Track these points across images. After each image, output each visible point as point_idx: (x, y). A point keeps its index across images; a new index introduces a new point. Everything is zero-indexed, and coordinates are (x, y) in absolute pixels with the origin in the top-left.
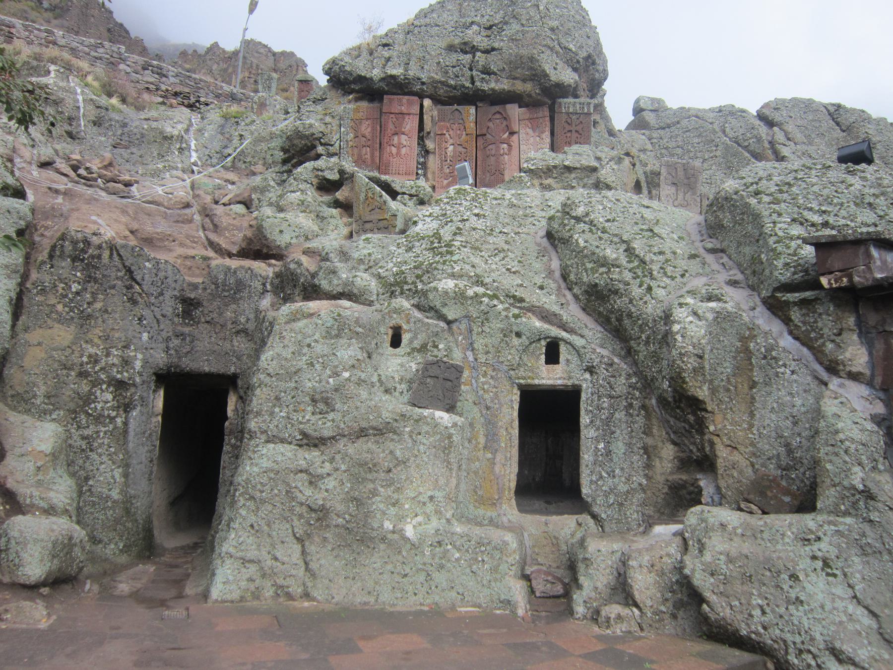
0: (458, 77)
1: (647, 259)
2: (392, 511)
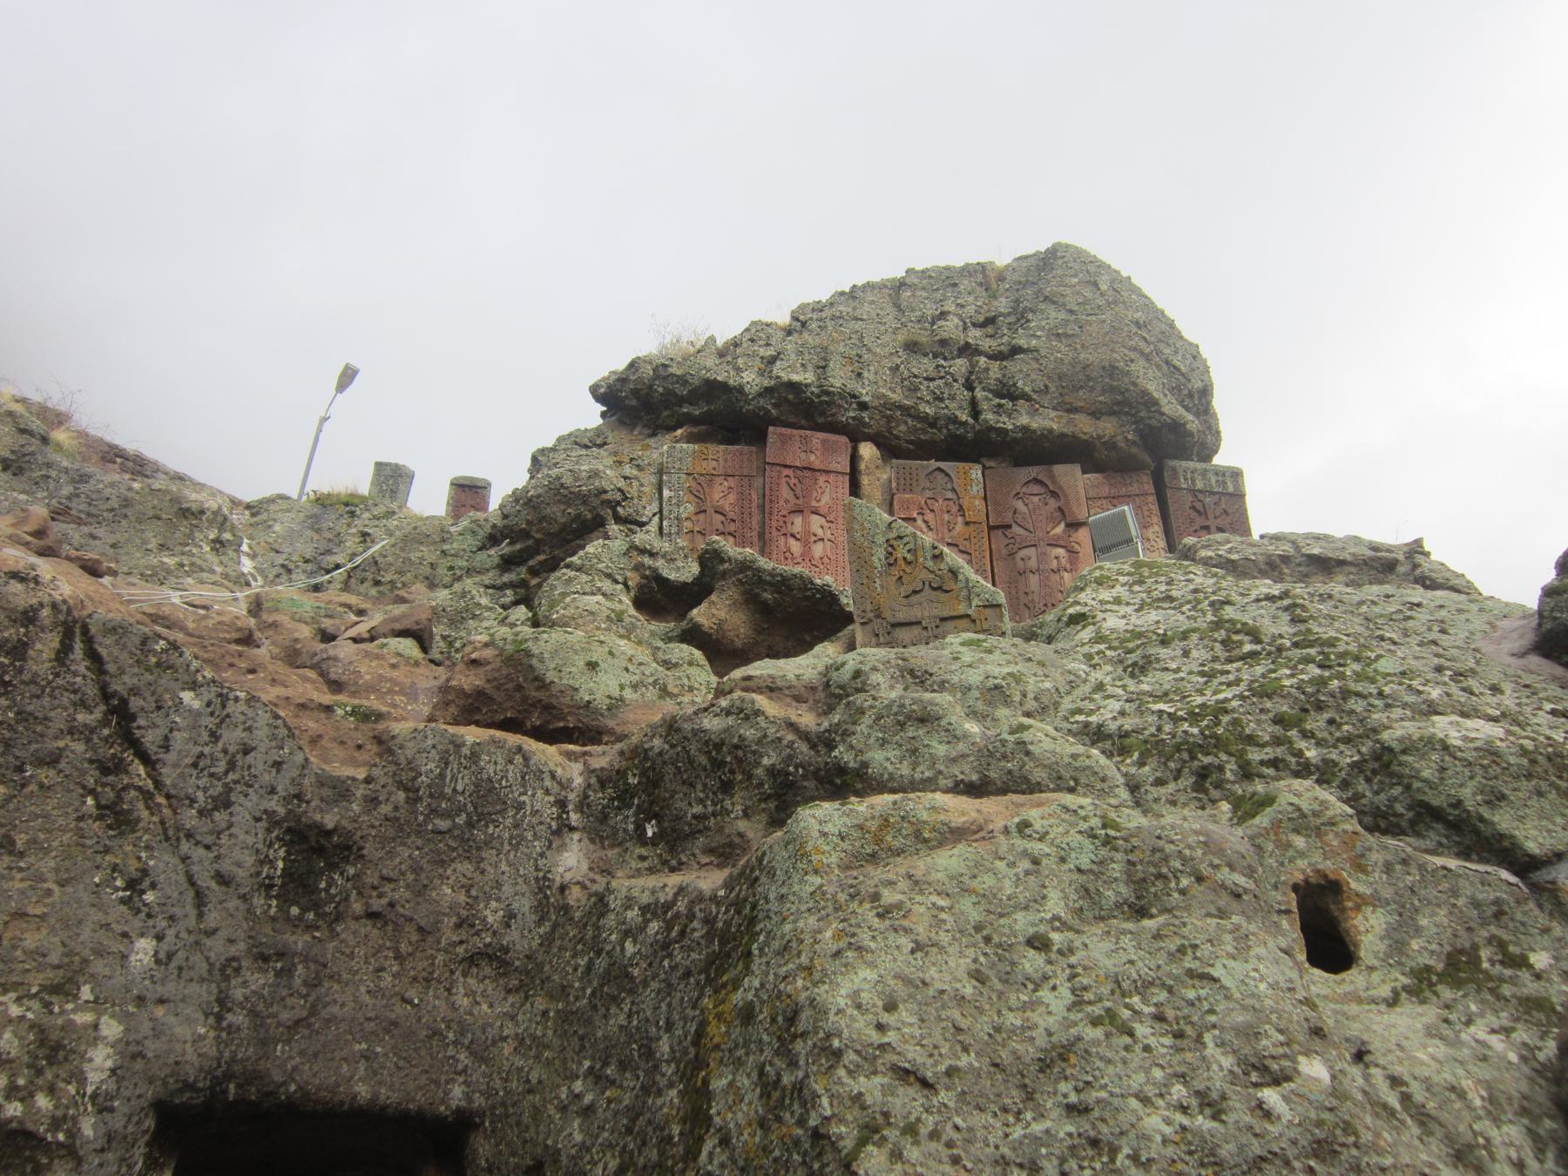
0: (941, 400)
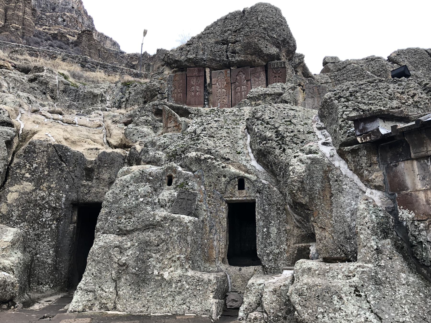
1: (285, 135)
2: (158, 265)
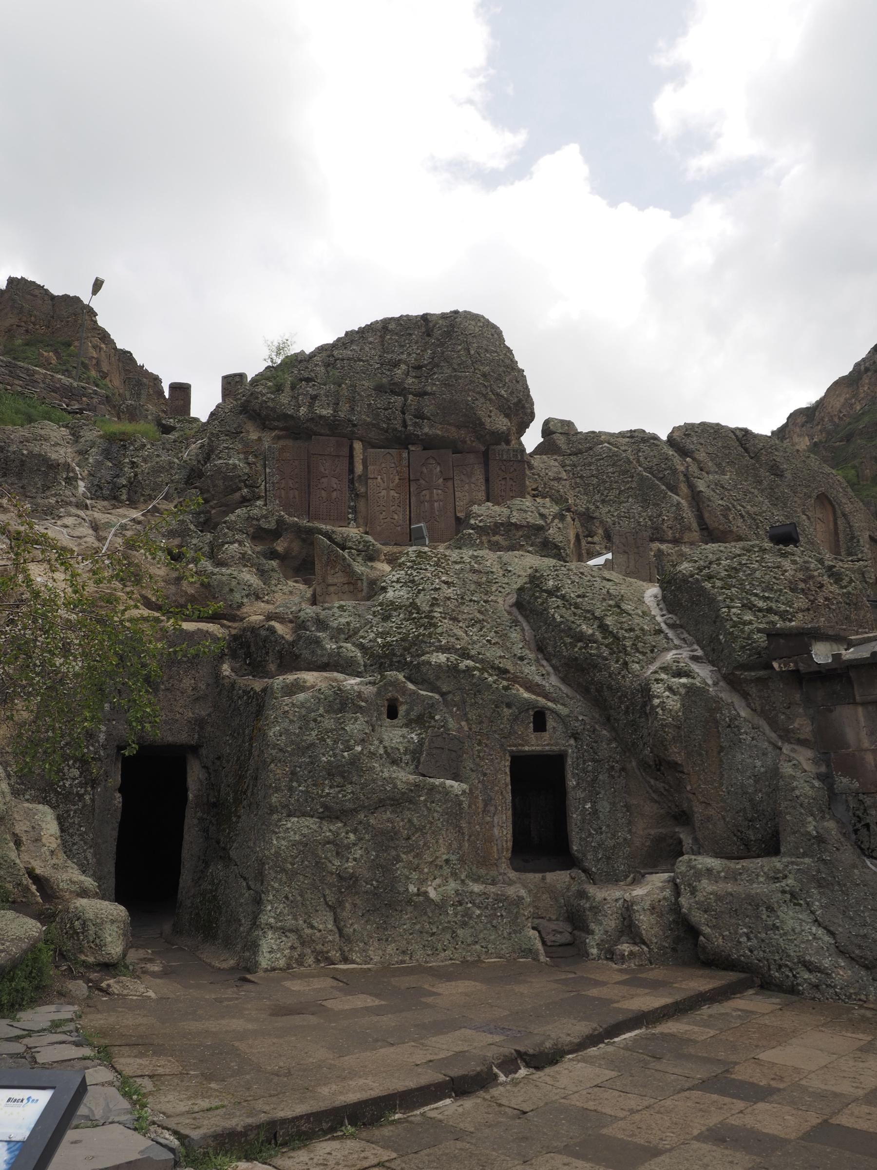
1: (620, 635)
2: (415, 875)
